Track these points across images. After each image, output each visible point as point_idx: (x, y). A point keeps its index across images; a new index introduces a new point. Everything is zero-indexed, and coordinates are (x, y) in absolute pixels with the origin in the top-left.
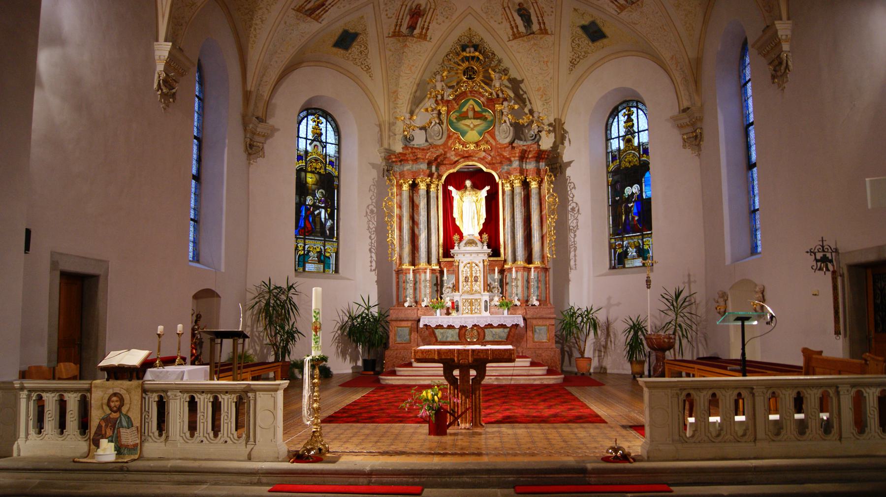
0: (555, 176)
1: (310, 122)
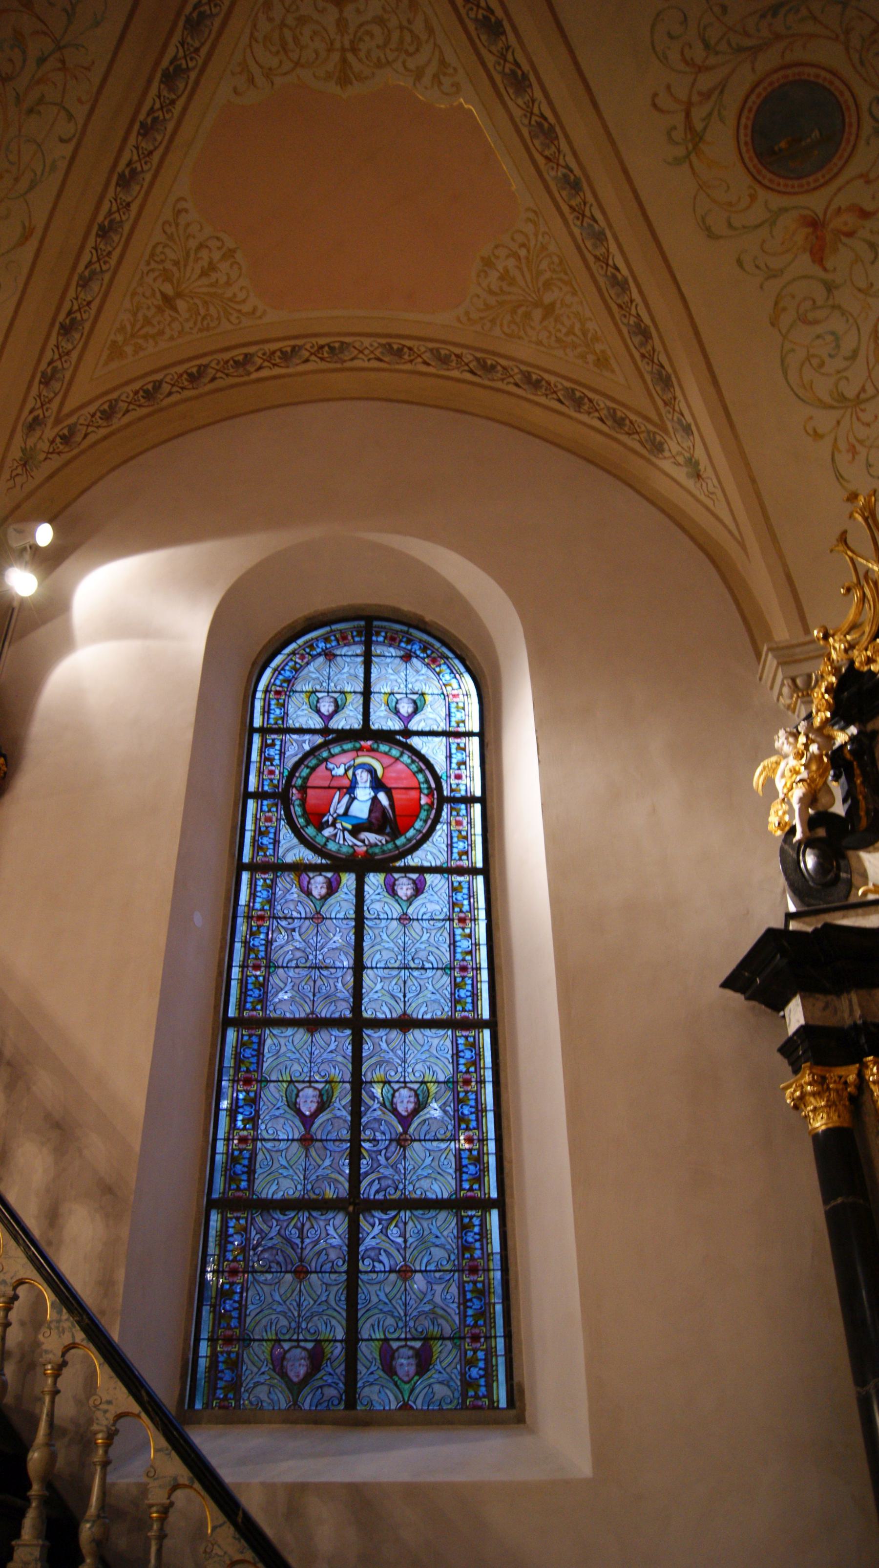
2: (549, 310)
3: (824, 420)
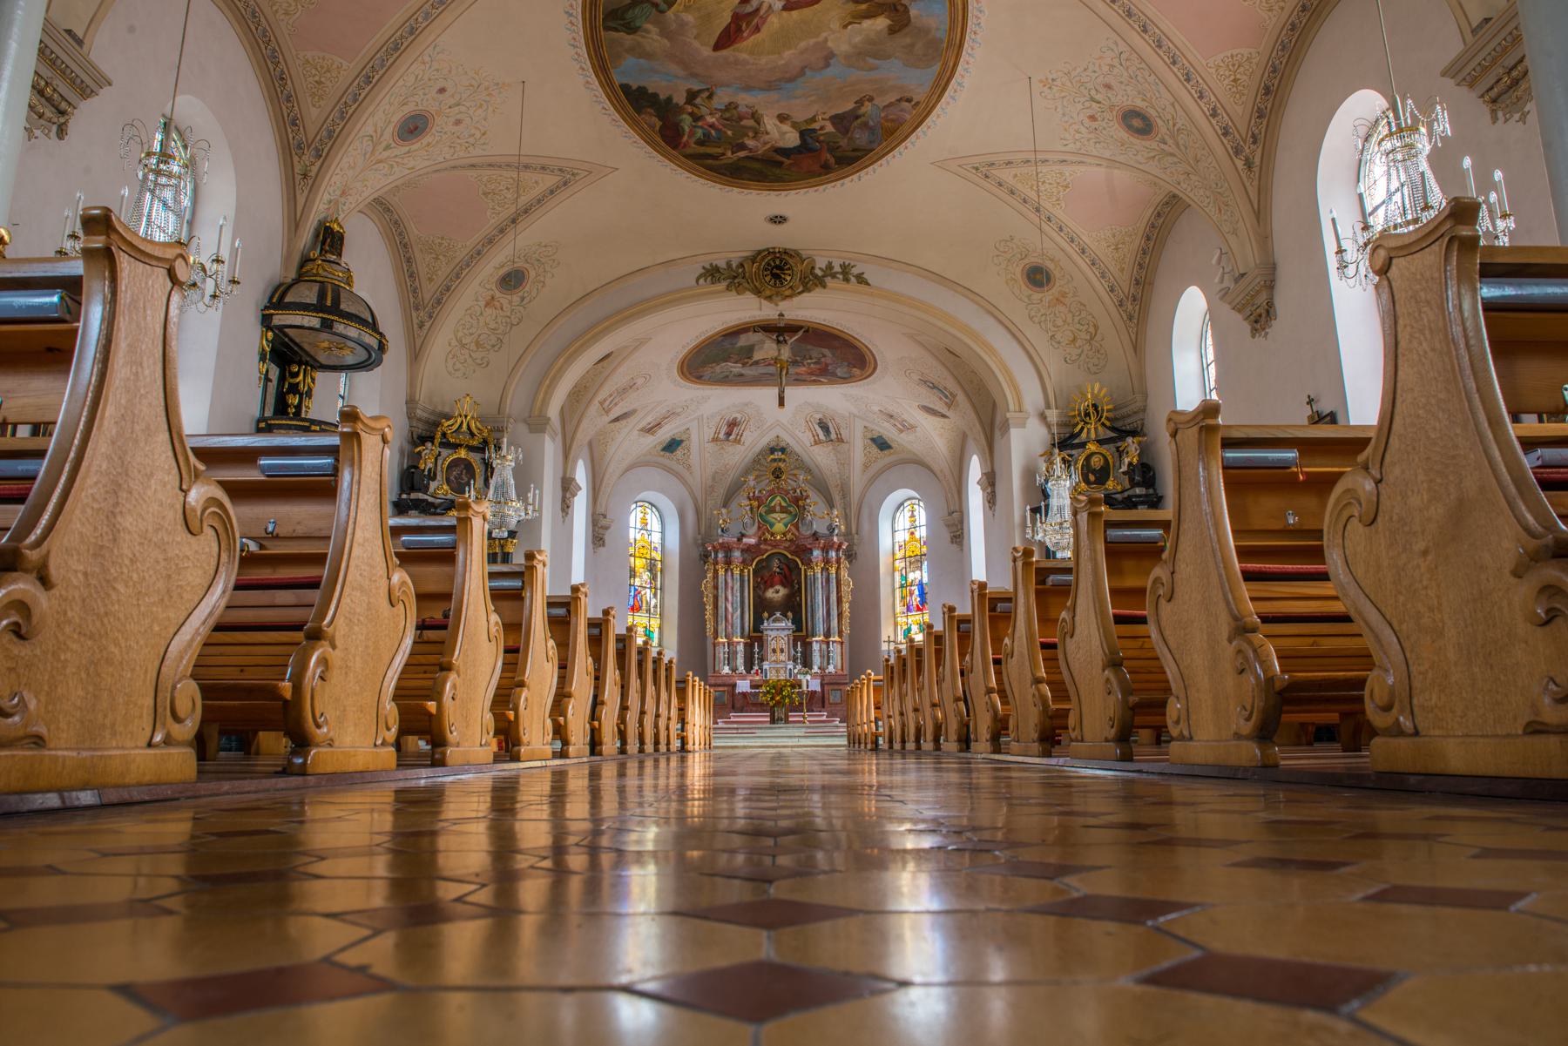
0: (850, 563)
1: (639, 513)
2: (437, 258)
3: (454, 342)
